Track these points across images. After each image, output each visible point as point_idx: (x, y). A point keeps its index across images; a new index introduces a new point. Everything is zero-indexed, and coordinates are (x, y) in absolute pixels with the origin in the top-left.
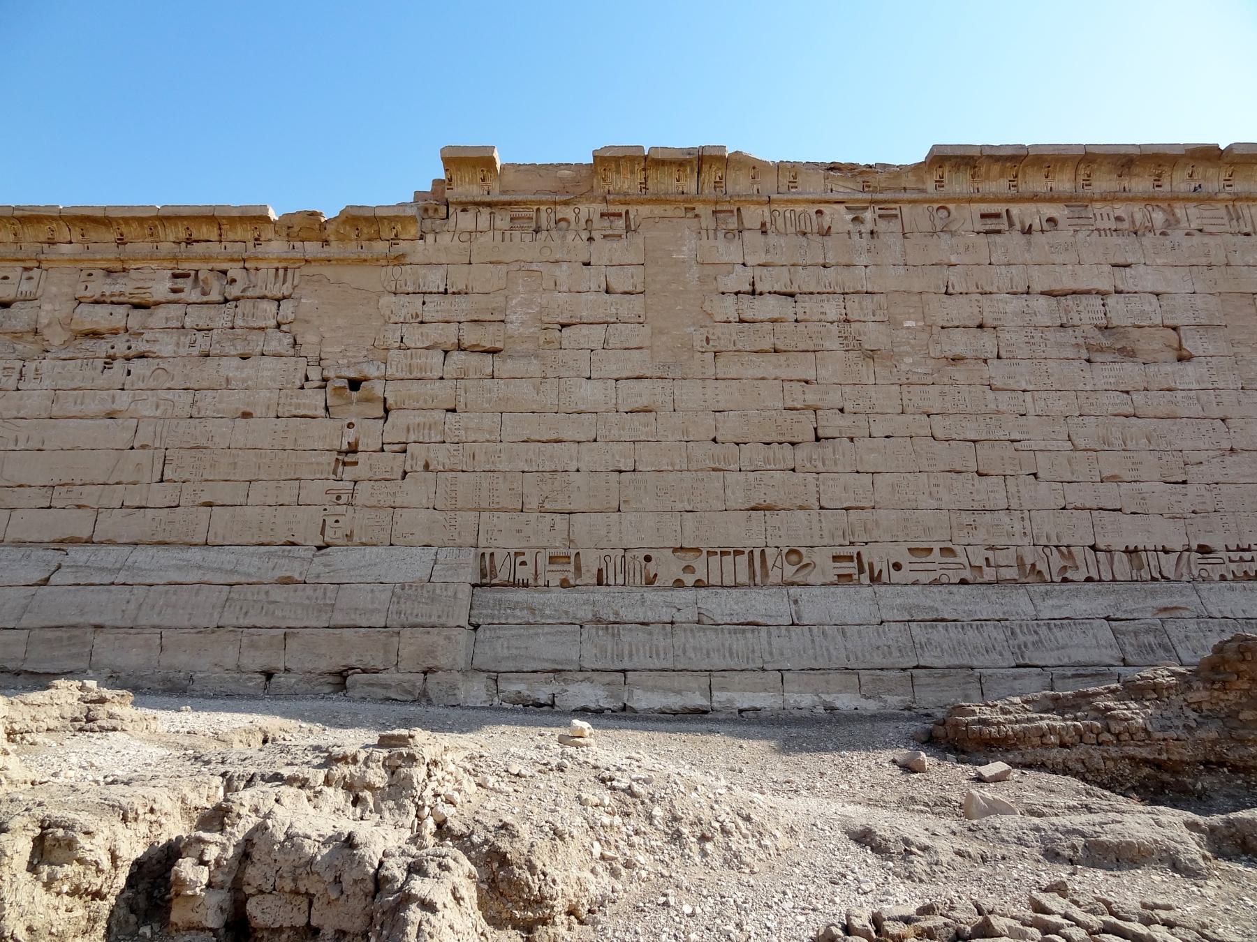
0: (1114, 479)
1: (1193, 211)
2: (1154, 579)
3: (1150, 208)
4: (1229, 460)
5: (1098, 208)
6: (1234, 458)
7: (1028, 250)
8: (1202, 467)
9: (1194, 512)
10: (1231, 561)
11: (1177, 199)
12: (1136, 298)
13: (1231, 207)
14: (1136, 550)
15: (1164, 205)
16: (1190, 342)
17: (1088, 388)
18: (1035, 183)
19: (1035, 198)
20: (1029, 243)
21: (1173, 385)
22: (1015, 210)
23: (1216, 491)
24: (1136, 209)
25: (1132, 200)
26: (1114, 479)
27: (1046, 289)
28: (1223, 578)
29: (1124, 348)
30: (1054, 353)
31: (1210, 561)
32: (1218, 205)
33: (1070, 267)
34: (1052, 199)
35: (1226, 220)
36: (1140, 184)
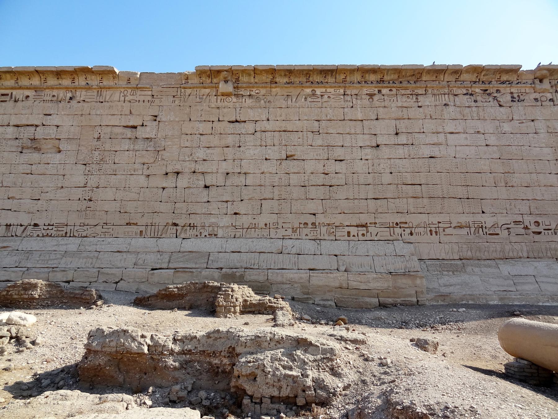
0: (13, 198)
1: (84, 93)
2: (12, 236)
3: (67, 92)
4: (59, 191)
5: (48, 92)
6: (62, 190)
7: (13, 109)
8: (47, 194)
9: (38, 211)
10: (44, 229)
11: (104, 88)
12: (48, 128)
13: (99, 92)
14: (10, 225)
15: (73, 91)
16: (63, 145)
17: (16, 163)
18: (24, 82)
19: (20, 88)
20: (15, 106)
21: (49, 162)
22: (14, 92)
23: (50, 203)
24: (62, 92)
25: (60, 88)
26: (13, 198)
27: (15, 124)
28: (38, 236)
29: (37, 147)
30: (8, 149)
31: (36, 229)
32: (95, 91)
33: (27, 115)
34: (28, 88)
35: (95, 97)
36: (66, 82)
